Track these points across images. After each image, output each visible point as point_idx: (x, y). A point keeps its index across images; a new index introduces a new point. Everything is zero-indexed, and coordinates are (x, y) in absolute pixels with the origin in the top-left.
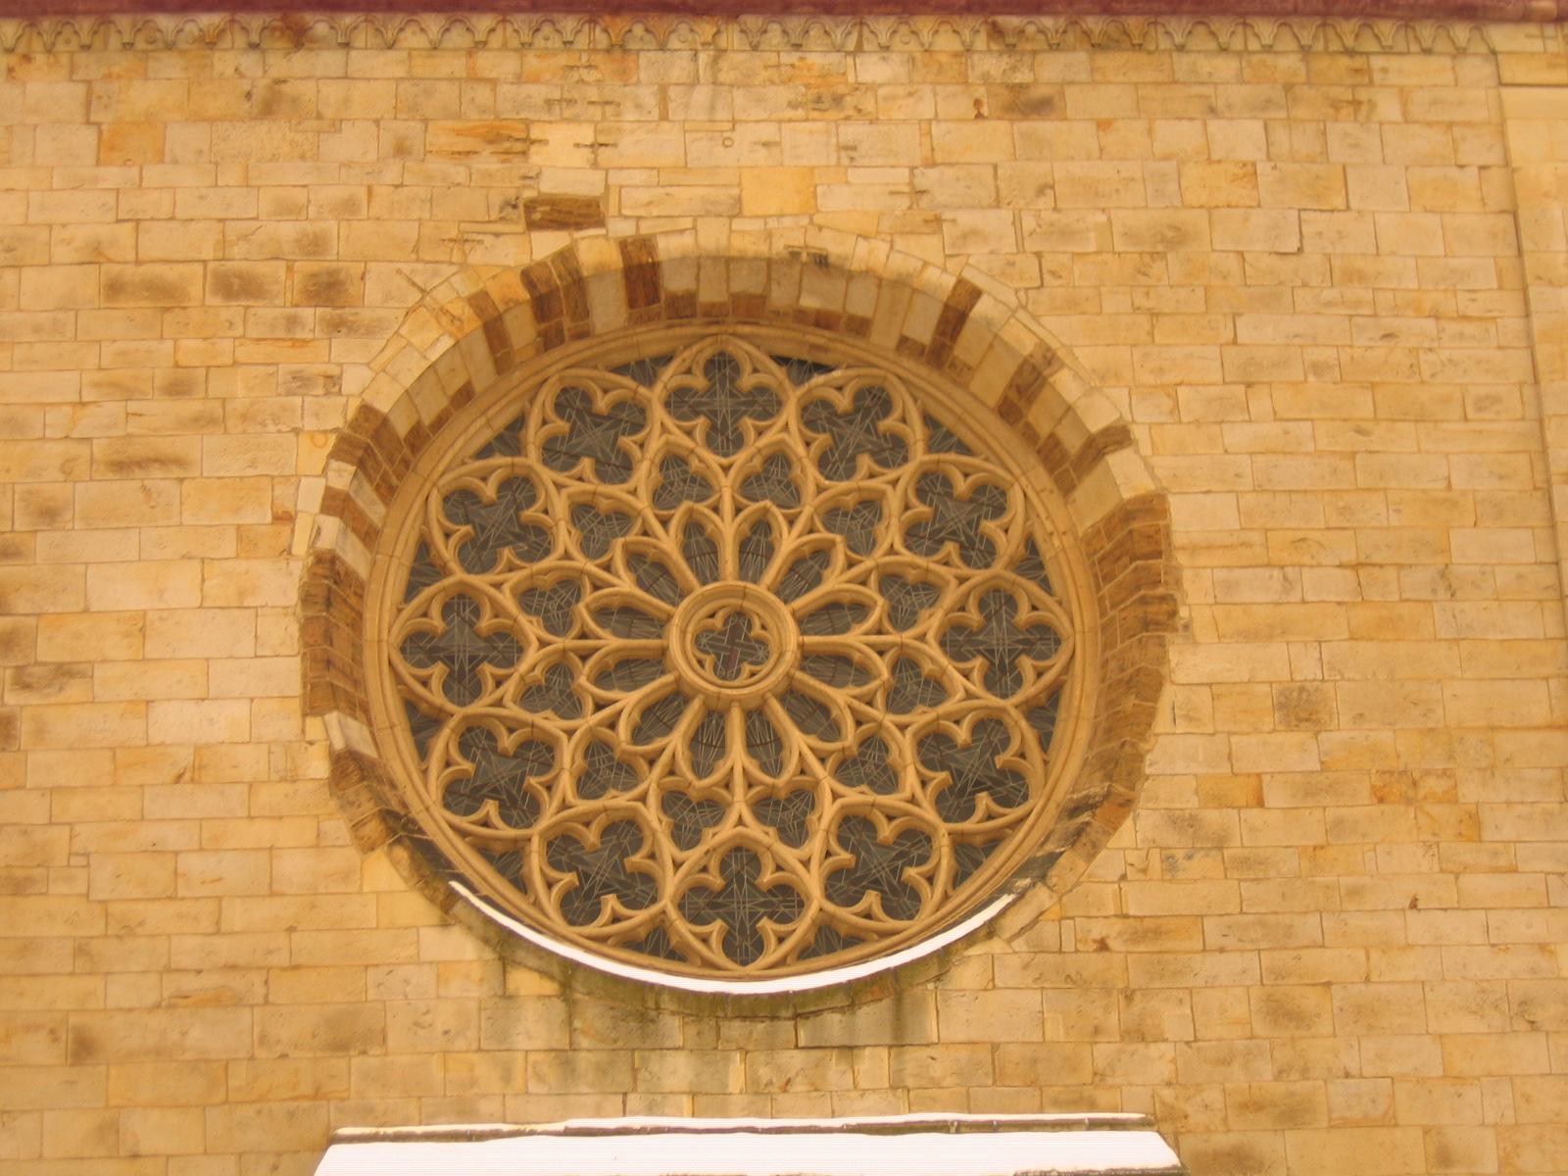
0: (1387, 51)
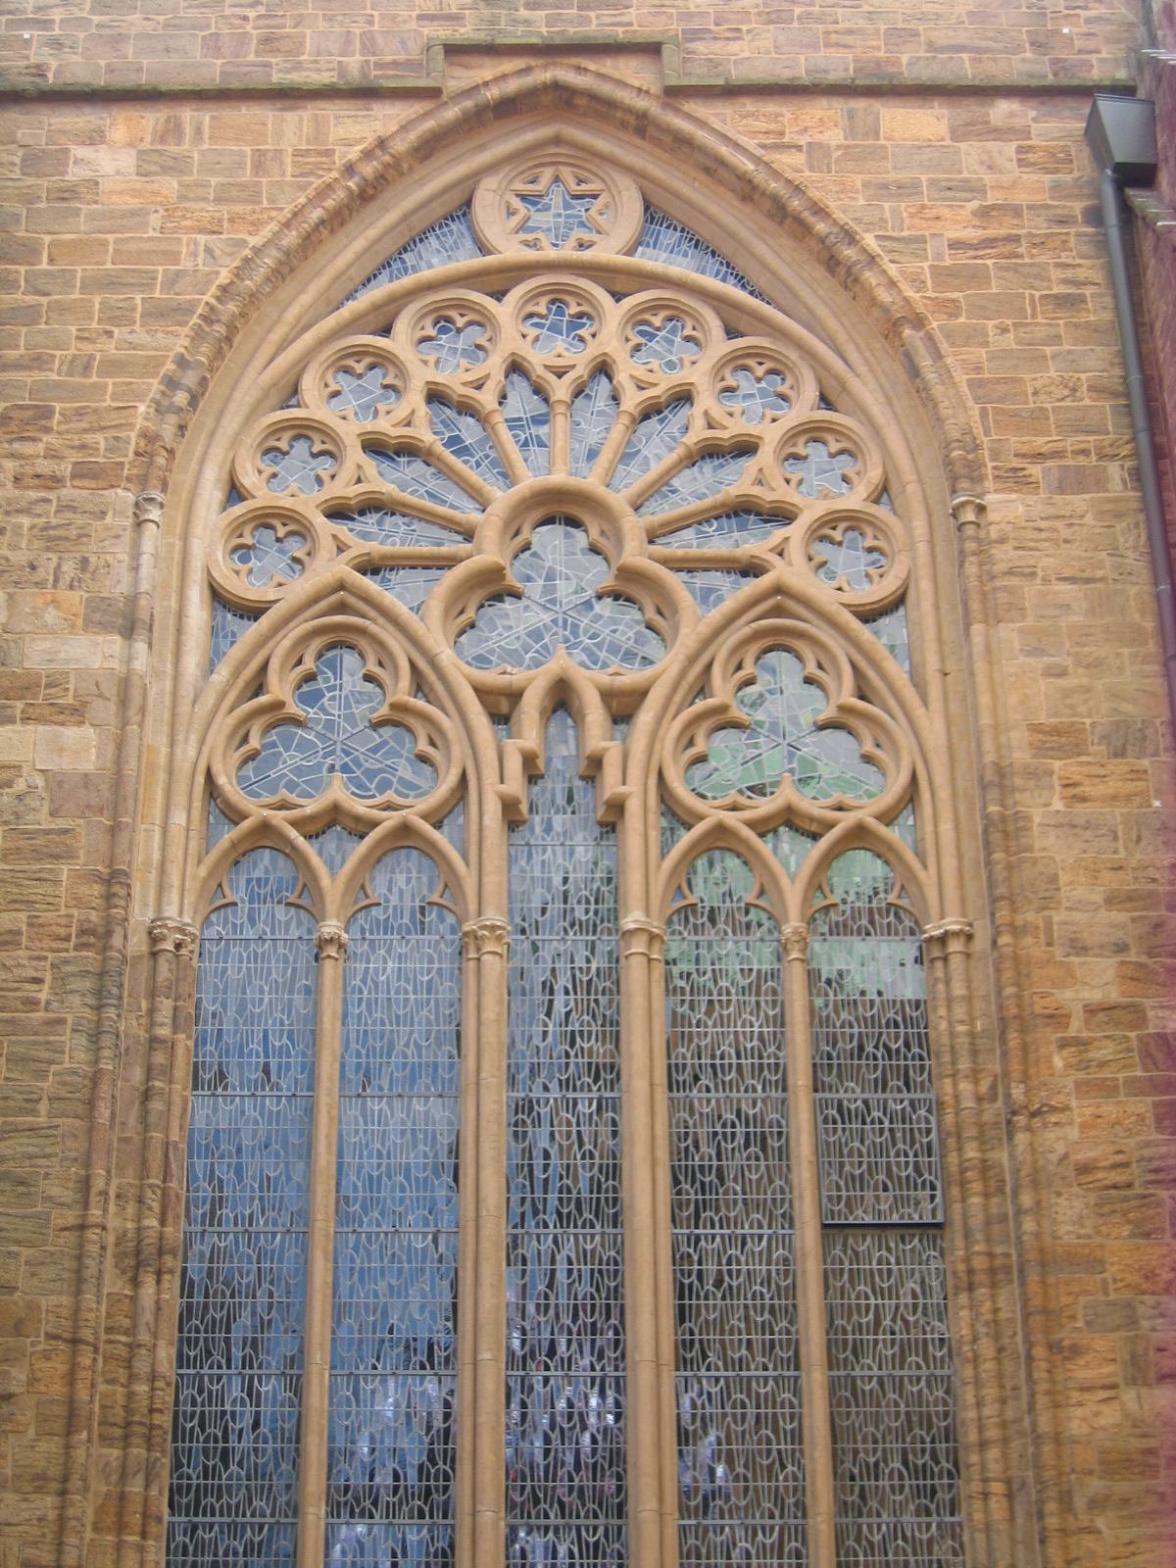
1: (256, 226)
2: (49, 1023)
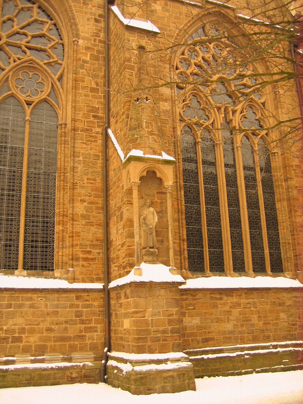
1: (181, 24)
2: (168, 150)
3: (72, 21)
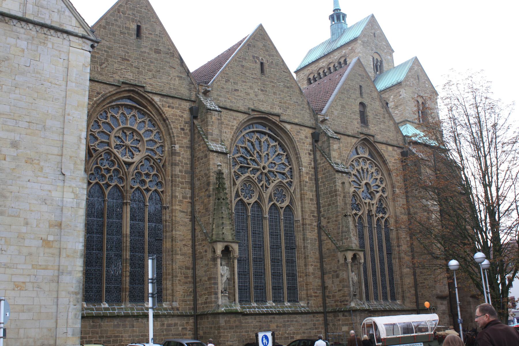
0: (51, 35)
3: (299, 155)
